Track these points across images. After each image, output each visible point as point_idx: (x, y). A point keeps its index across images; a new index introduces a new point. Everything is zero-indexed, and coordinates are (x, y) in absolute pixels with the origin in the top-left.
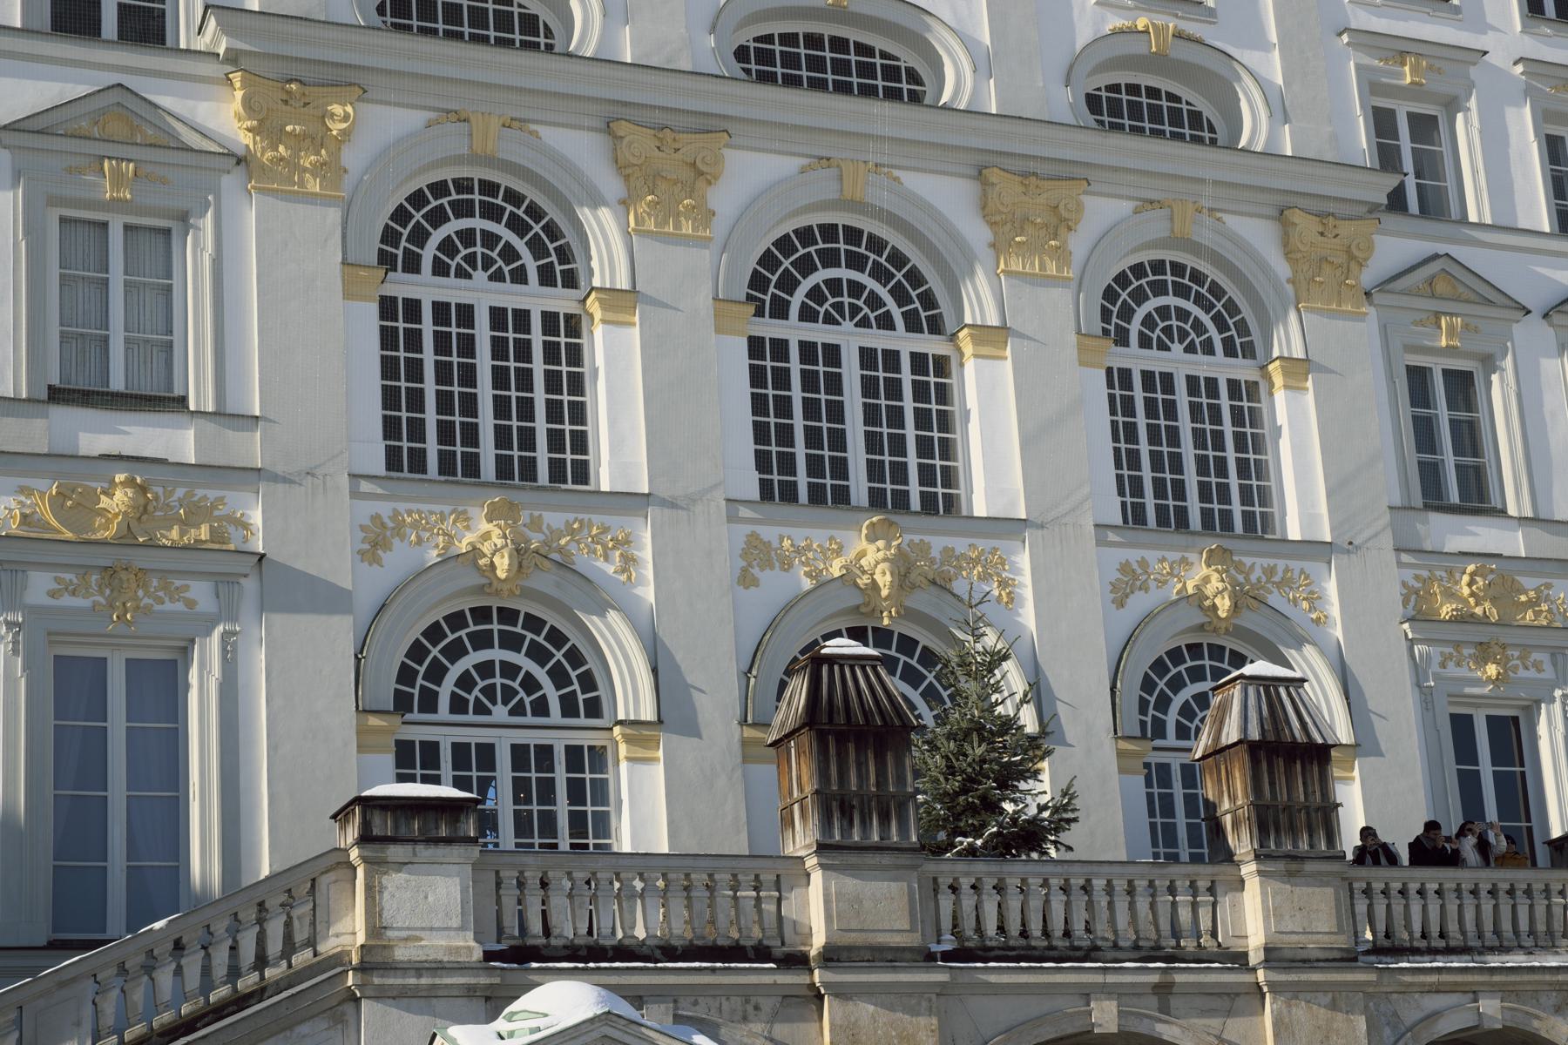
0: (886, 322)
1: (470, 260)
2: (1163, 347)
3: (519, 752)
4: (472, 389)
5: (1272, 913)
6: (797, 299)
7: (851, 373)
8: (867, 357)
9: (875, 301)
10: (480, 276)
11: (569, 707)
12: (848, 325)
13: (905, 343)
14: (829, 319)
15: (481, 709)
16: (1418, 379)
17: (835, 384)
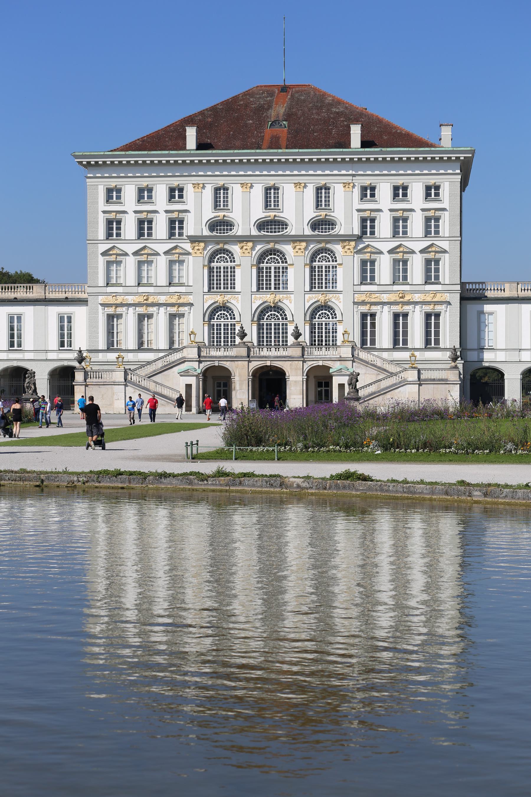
0: (279, 263)
1: (221, 260)
2: (322, 262)
3: (224, 325)
4: (219, 279)
5: (292, 352)
6: (265, 261)
7: (273, 270)
8: (275, 268)
9: (277, 260)
10: (222, 262)
11: (231, 318)
12: (273, 264)
13: (281, 265)
14: (270, 263)
15: (220, 319)
16: (364, 263)
17: (270, 272)
